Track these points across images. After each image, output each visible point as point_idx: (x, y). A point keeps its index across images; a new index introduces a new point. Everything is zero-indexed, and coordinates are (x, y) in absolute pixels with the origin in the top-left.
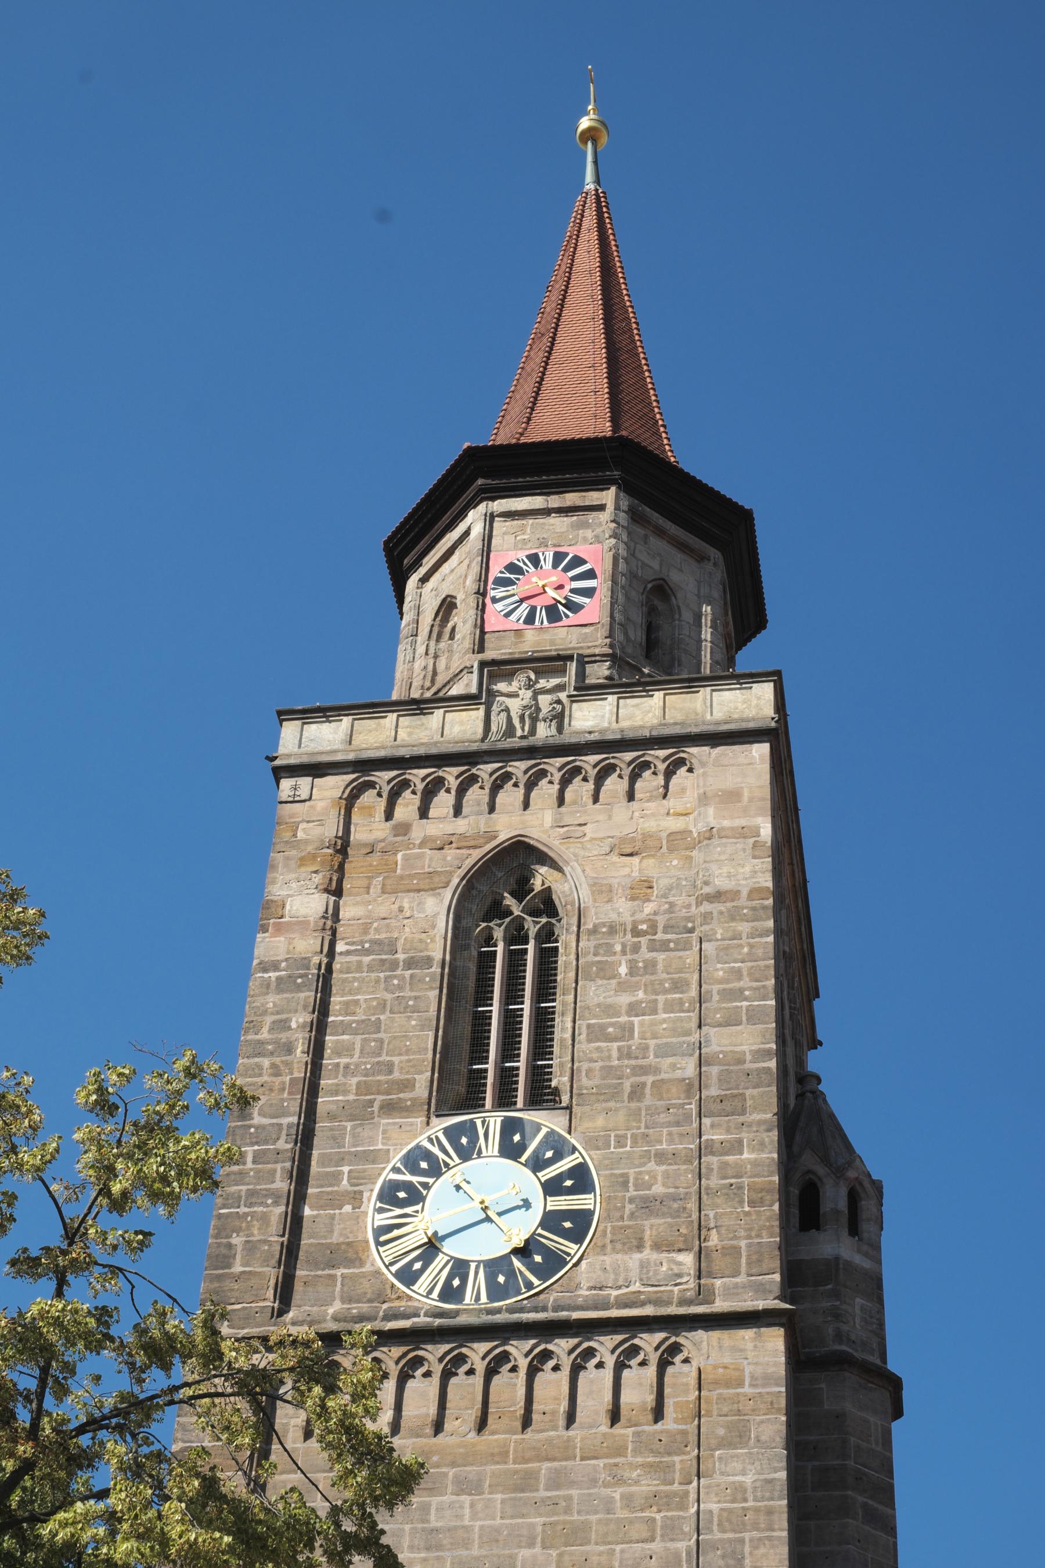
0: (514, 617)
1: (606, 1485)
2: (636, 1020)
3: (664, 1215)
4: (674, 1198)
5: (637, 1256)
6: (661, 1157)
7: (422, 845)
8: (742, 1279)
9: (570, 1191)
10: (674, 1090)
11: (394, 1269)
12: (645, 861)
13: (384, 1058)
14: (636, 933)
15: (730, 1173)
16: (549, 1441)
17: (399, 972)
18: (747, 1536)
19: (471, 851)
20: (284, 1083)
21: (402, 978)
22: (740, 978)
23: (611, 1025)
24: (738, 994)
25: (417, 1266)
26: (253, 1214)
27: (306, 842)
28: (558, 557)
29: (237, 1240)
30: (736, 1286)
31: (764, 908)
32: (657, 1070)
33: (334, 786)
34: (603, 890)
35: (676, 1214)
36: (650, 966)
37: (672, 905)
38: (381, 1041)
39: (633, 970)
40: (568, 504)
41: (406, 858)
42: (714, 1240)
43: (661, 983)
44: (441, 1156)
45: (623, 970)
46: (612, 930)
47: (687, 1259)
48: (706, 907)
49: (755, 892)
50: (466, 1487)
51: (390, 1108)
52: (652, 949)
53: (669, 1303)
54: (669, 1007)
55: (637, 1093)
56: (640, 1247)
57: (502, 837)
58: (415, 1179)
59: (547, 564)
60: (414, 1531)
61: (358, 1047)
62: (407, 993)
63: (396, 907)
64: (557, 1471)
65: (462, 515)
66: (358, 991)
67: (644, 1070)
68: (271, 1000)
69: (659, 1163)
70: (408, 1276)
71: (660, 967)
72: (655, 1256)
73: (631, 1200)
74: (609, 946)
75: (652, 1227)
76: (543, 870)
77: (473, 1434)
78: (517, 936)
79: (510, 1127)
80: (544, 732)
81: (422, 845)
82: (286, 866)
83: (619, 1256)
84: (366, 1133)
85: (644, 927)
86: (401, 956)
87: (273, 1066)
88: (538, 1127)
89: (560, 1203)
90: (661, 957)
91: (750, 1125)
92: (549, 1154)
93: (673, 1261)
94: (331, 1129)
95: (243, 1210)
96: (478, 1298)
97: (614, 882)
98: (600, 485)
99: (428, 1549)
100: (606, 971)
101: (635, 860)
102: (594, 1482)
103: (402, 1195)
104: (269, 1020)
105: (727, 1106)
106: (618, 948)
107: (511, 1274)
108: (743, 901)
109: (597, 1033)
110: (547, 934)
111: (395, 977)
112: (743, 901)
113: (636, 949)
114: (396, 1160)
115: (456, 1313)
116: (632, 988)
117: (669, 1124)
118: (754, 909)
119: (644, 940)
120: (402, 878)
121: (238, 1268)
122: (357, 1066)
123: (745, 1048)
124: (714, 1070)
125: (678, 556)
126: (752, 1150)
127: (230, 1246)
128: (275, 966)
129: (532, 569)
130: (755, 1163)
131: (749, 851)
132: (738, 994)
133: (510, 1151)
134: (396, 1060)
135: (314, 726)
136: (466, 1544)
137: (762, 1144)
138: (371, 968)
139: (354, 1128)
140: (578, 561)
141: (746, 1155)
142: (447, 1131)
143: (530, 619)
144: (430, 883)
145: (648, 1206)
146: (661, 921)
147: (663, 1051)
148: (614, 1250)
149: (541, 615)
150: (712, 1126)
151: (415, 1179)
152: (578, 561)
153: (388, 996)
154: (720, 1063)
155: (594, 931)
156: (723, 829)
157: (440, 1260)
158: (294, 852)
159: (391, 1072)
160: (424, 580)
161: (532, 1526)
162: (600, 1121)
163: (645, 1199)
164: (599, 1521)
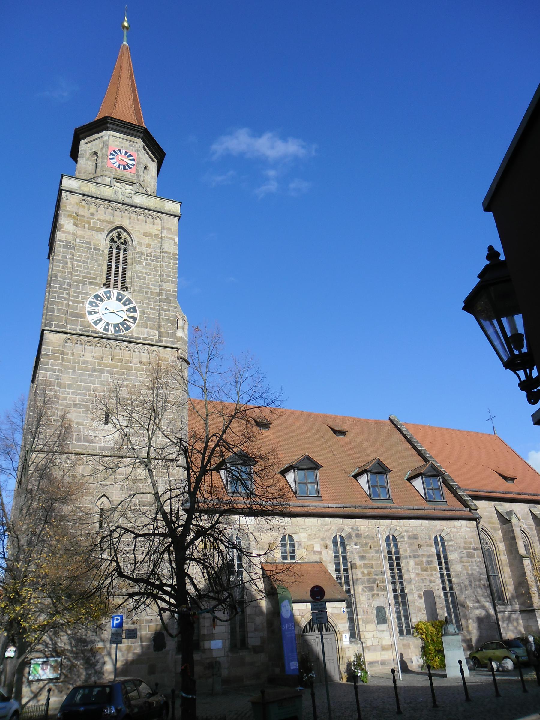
0: (115, 165)
1: (139, 377)
2: (147, 276)
3: (152, 322)
4: (155, 318)
5: (146, 330)
6: (152, 309)
7: (98, 220)
8: (169, 339)
12: (150, 239)
13: (89, 271)
14: (147, 256)
15: (167, 316)
16: (127, 366)
17: (92, 251)
21: (93, 252)
22: (170, 273)
24: (170, 276)
25: (98, 322)
26: (59, 302)
27: (69, 211)
28: (126, 153)
31: (176, 258)
32: (151, 289)
33: (75, 198)
34: (140, 244)
35: (155, 322)
36: (150, 265)
38: (88, 266)
39: (146, 265)
40: (129, 139)
41: (94, 222)
42: (162, 329)
43: (153, 269)
45: (144, 264)
46: (142, 254)
47: (157, 332)
48: (163, 254)
49: (174, 254)
51: (90, 283)
53: (153, 341)
54: (154, 275)
55: (147, 293)
56: (147, 328)
59: (123, 153)
60: (98, 380)
61: (83, 266)
62: (94, 256)
63: (91, 234)
65: (101, 131)
66: (82, 253)
68: (62, 250)
69: (151, 310)
70: (96, 323)
71: (152, 265)
72: (150, 330)
73: (145, 317)
75: (149, 323)
76: (125, 234)
78: (118, 248)
79: (119, 294)
81: (98, 220)
82: (64, 216)
84: (85, 288)
85: (149, 255)
86: (93, 247)
87: (63, 266)
90: (153, 263)
91: (171, 306)
92: (127, 303)
93: (153, 332)
94: (77, 285)
95: (56, 300)
96: (112, 332)
97: (143, 242)
98: (137, 137)
101: (147, 238)
104: (61, 255)
105: (167, 301)
106: (143, 258)
107: (119, 328)
108: (171, 255)
109: (138, 277)
113: (147, 260)
114: (92, 296)
115: (108, 334)
116: (146, 269)
118: (173, 257)
119: (149, 258)
121: (56, 314)
122: (83, 271)
123: (171, 289)
125: (150, 160)
126: (172, 312)
127: (54, 308)
128: (62, 241)
129: (120, 154)
130: (172, 315)
131: (173, 244)
132: (170, 276)
133: (119, 300)
135: (71, 181)
137: (174, 311)
138: (85, 248)
139: (82, 286)
140: (130, 155)
141: (170, 313)
142: (104, 292)
143: (119, 167)
144: (101, 230)
145: (148, 319)
146: (153, 254)
148: (141, 327)
149: (122, 167)
150: (164, 304)
152: (130, 155)
153: (90, 256)
155: (138, 253)
157: (102, 322)
158: (66, 213)
159: (91, 275)
160: (87, 143)
162: (138, 298)
163: (148, 317)
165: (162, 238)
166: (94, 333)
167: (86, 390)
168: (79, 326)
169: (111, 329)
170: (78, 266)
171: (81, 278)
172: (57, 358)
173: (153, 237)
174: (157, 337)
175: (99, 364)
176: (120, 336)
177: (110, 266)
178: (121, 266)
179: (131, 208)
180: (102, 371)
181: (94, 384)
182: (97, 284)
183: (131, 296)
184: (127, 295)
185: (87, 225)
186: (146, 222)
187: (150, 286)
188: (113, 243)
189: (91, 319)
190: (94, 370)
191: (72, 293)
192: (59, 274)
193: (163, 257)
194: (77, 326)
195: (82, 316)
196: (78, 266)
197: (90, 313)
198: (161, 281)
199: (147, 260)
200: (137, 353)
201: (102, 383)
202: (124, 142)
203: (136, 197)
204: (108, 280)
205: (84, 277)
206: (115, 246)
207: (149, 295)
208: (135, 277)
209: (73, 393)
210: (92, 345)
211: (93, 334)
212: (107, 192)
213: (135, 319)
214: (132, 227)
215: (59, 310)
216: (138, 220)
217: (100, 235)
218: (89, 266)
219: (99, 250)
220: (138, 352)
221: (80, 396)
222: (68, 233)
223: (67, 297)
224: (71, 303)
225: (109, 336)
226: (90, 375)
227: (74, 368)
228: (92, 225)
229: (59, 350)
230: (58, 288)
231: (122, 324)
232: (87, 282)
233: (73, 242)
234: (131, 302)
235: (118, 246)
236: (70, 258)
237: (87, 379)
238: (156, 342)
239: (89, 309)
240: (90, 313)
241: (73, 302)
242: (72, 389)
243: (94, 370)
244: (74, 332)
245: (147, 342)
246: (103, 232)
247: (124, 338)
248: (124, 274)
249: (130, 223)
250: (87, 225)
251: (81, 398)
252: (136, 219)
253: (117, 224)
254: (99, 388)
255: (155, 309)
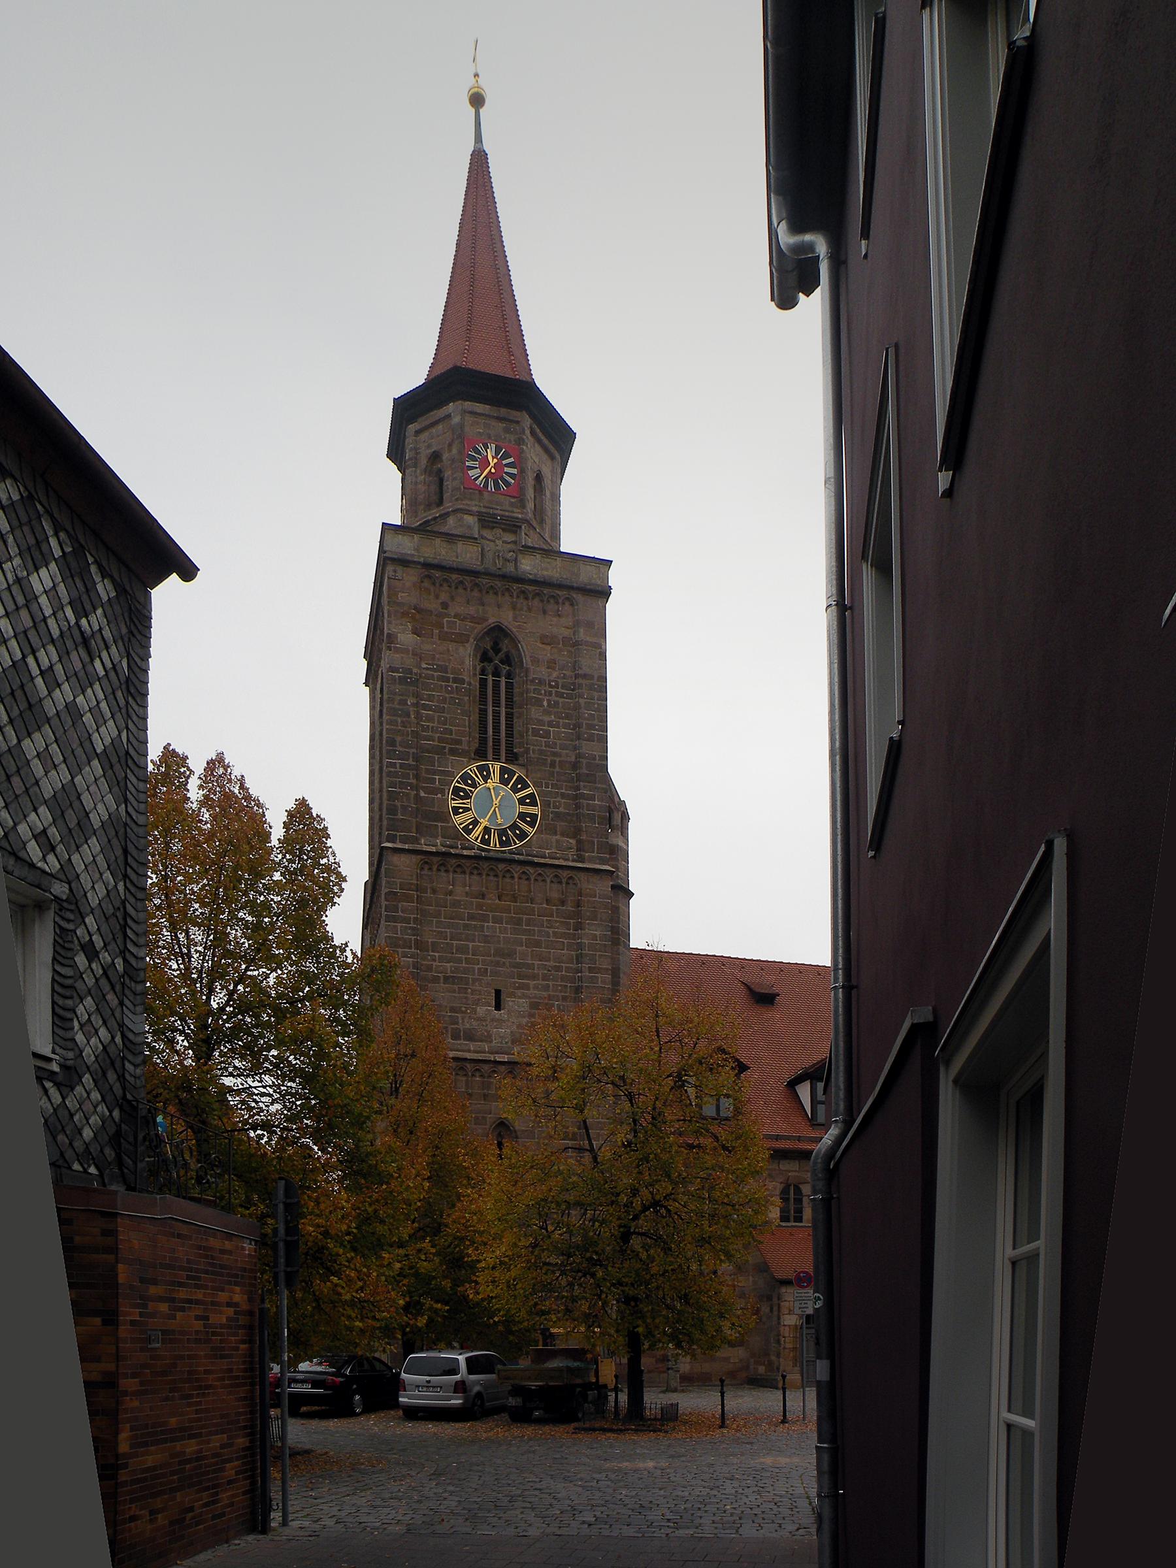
5: (555, 838)
6: (563, 796)
9: (527, 804)
10: (567, 765)
11: (461, 826)
14: (551, 686)
18: (598, 953)
19: (477, 625)
20: (408, 731)
21: (451, 687)
23: (542, 730)
26: (403, 792)
29: (397, 803)
30: (593, 857)
34: (535, 661)
36: (557, 703)
37: (564, 674)
38: (446, 718)
44: (476, 779)
45: (545, 703)
46: (541, 682)
48: (580, 681)
50: (497, 920)
51: (453, 752)
52: (557, 696)
54: (566, 726)
55: (553, 765)
56: (555, 834)
57: (490, 621)
58: (466, 788)
60: (479, 935)
61: (436, 718)
64: (530, 919)
67: (555, 754)
73: (552, 812)
74: (540, 690)
75: (561, 825)
77: (497, 901)
80: (510, 568)
81: (455, 616)
83: (548, 836)
87: (402, 722)
88: (515, 773)
89: (523, 809)
90: (561, 700)
99: (485, 942)
100: (539, 703)
101: (548, 648)
102: (542, 926)
103: (462, 794)
104: (398, 698)
106: (543, 692)
107: (507, 836)
108: (595, 681)
109: (536, 733)
110: (509, 676)
111: (449, 686)
112: (595, 681)
113: (550, 694)
116: (549, 713)
117: (566, 781)
119: (553, 690)
120: (446, 632)
122: (437, 728)
124: (584, 761)
127: (395, 806)
130: (600, 806)
134: (453, 728)
136: (499, 942)
144: (461, 639)
145: (558, 816)
147: (563, 747)
151: (466, 788)
153: (447, 695)
154: (586, 758)
155: (533, 681)
156: (588, 642)
159: (452, 735)
161: (522, 939)
164: (545, 940)
165: (576, 644)
166: (466, 848)
167: (462, 953)
168: (440, 837)
169: (494, 839)
170: (430, 719)
171: (436, 743)
172: (408, 899)
173: (559, 644)
174: (573, 852)
175: (480, 907)
176: (511, 852)
177: (483, 713)
178: (503, 711)
179: (515, 586)
180: (484, 918)
181: (474, 941)
182: (463, 754)
183: (525, 771)
184: (519, 772)
185: (436, 631)
186: (545, 612)
187: (558, 750)
188: (485, 664)
189: (460, 820)
190: (471, 917)
191: (424, 774)
192: (398, 739)
193: (580, 685)
194: (437, 837)
195: (444, 817)
196: (430, 719)
197: (456, 811)
198: (579, 738)
199: (550, 694)
200: (541, 884)
201: (486, 939)
202: (493, 424)
203: (524, 558)
204: (483, 741)
205: (440, 740)
206: (490, 669)
207: (557, 769)
208: (530, 733)
209: (441, 959)
210: (464, 872)
211: (465, 852)
212: (467, 555)
213: (534, 817)
214: (519, 627)
215: (404, 808)
216: (530, 610)
217: (461, 649)
218: (448, 716)
219: (462, 681)
220: (543, 880)
221: (452, 964)
222: (406, 651)
223: (414, 781)
224: (422, 794)
225: (492, 854)
226: (466, 926)
227: (438, 915)
228: (445, 629)
229: (412, 884)
230: (398, 766)
231: (514, 827)
232: (447, 750)
233: (415, 670)
234: (526, 786)
235: (496, 668)
236: (413, 704)
237: (461, 934)
238: (573, 861)
239: (454, 804)
240: (456, 811)
241: (426, 790)
242: (438, 952)
243: (471, 917)
244: (434, 849)
245: (556, 862)
246: (468, 641)
247: (516, 857)
248: (510, 726)
249: (515, 618)
250: (436, 631)
251: (454, 967)
252: (525, 608)
253: (492, 620)
254: (481, 949)
255: (568, 795)
